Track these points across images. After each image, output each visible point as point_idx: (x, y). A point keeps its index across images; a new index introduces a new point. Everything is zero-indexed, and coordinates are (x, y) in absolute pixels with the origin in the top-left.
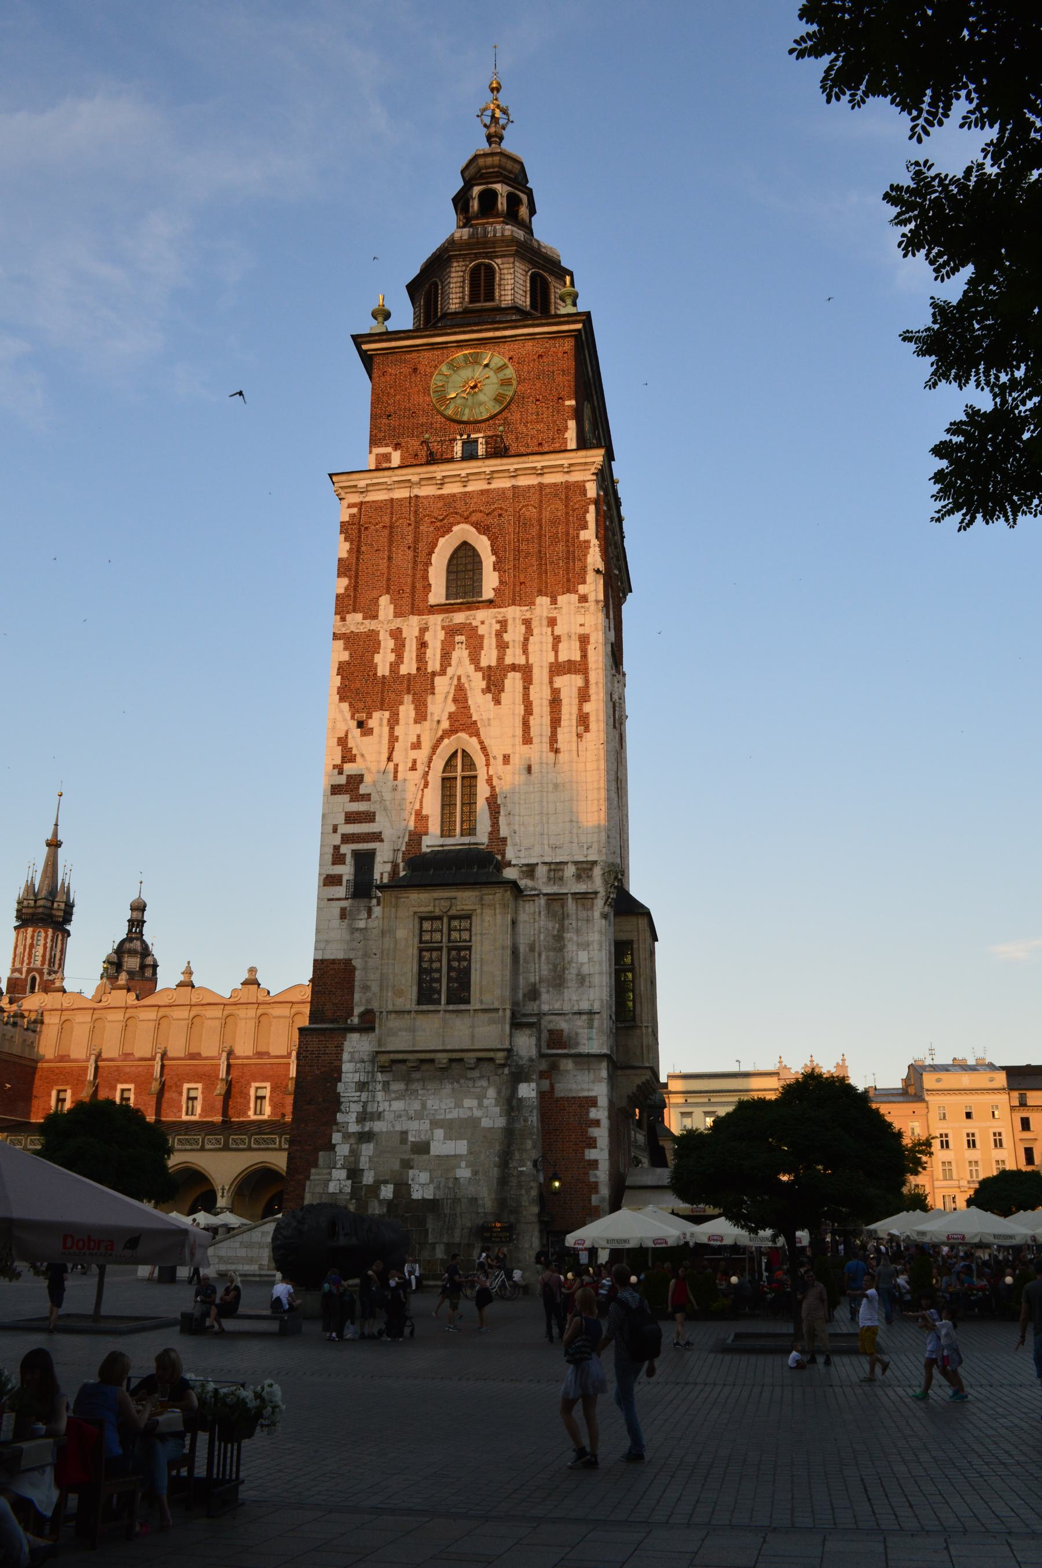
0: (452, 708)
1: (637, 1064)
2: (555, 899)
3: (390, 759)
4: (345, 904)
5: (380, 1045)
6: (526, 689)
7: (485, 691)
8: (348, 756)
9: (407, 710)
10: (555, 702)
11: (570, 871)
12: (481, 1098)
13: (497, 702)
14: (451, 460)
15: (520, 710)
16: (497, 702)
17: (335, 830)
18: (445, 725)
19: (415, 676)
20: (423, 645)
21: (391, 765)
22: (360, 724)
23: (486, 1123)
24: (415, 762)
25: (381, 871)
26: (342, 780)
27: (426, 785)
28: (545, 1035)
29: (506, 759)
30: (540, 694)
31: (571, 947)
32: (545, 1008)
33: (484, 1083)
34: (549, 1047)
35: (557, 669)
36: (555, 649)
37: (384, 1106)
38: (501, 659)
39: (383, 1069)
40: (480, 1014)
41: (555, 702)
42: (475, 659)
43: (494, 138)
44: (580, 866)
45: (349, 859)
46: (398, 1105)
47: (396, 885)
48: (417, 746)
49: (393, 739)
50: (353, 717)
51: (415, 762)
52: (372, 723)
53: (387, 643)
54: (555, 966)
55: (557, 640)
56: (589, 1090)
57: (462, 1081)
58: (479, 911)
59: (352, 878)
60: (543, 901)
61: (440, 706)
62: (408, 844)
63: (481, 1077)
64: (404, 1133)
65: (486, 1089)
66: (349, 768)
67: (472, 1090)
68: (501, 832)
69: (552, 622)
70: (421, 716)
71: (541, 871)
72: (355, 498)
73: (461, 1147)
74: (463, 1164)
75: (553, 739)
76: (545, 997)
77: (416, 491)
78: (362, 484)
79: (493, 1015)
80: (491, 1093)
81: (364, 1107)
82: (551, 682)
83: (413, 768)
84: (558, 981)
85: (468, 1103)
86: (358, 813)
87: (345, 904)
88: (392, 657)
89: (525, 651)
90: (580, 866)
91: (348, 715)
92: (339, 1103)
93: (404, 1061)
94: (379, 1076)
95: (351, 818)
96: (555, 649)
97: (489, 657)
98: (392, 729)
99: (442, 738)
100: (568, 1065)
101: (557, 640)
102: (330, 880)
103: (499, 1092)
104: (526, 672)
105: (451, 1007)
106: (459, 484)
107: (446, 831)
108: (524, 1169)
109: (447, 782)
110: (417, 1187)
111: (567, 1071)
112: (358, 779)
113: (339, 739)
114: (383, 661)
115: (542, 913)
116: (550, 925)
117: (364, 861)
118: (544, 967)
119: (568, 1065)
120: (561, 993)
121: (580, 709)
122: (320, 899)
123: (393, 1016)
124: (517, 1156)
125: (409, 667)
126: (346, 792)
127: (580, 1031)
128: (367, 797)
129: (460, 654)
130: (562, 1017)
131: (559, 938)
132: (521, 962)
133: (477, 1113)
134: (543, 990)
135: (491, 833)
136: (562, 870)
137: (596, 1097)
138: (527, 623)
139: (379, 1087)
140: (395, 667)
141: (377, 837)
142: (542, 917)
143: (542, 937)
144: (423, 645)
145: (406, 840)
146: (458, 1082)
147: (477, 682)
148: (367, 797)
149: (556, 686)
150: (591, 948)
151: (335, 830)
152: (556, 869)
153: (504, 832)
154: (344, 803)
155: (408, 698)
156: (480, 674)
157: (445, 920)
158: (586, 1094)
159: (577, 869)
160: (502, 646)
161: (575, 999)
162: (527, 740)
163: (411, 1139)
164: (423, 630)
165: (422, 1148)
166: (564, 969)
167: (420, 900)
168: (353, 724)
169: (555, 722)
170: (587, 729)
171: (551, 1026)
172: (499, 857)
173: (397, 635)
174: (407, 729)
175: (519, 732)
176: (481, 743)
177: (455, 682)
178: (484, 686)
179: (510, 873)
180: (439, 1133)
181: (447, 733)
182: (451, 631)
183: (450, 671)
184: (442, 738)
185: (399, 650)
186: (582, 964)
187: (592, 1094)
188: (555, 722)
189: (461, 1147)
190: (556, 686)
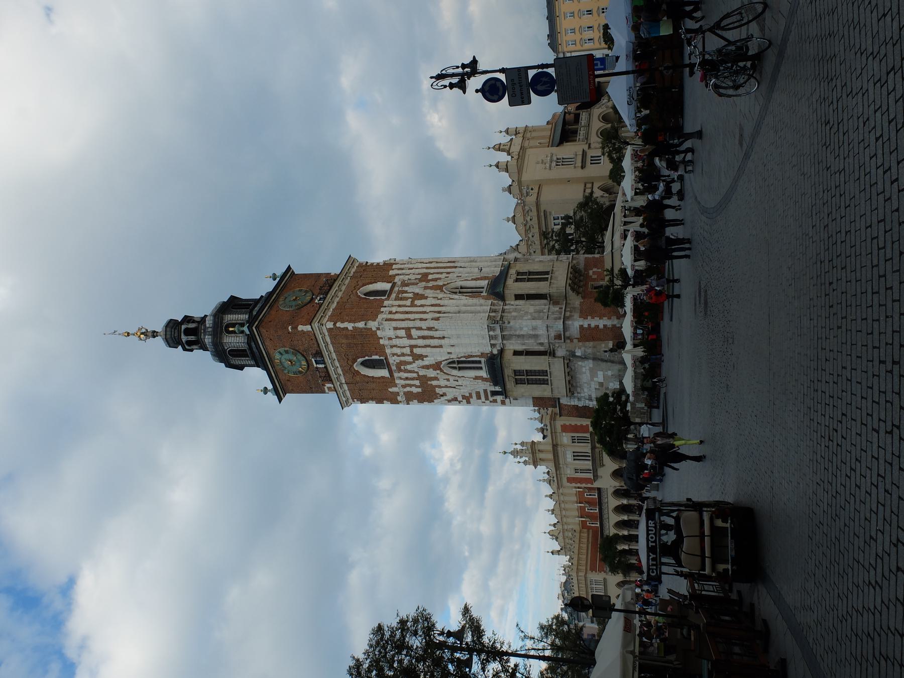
0: (431, 370)
1: (564, 294)
2: (503, 338)
3: (455, 388)
4: (511, 399)
5: (564, 396)
6: (419, 347)
7: (423, 360)
8: (455, 399)
9: (434, 383)
10: (424, 338)
11: (491, 333)
12: (582, 366)
13: (426, 356)
14: (326, 367)
15: (429, 349)
16: (426, 356)
17: (484, 402)
18: (438, 372)
19: (420, 381)
20: (407, 379)
21: (456, 387)
22: (442, 396)
23: (591, 366)
24: (454, 380)
25: (498, 389)
26: (465, 401)
27: (464, 377)
28: (557, 341)
29: (449, 353)
30: (421, 342)
31: (522, 333)
32: (546, 341)
33: (576, 365)
34: (561, 339)
35: (409, 336)
36: (401, 338)
37: (586, 394)
38: (409, 355)
39: (573, 394)
40: (551, 368)
41: (424, 338)
42: (410, 363)
43: (154, 334)
44: (490, 330)
45: (495, 397)
46: (586, 390)
47: (504, 386)
48: (448, 380)
49: (446, 387)
50: (440, 398)
51: (454, 380)
52: (441, 393)
53: (408, 389)
54: (530, 337)
55: (397, 337)
56: (577, 328)
58: (512, 368)
59: (501, 397)
60: (505, 342)
61: (431, 373)
63: (574, 366)
64: (596, 389)
66: (460, 398)
69: (390, 339)
70: (436, 379)
71: (493, 342)
72: (351, 400)
73: (600, 374)
74: (606, 373)
75: (439, 338)
77: (343, 381)
78: (344, 399)
79: (551, 364)
80: (580, 363)
81: (587, 399)
82: (416, 339)
83: (457, 381)
84: (536, 336)
85: (584, 369)
86: (477, 396)
87: (511, 399)
88: (414, 388)
89: (404, 347)
90: (490, 330)
91: (439, 400)
92: (586, 406)
93: (570, 389)
94: (576, 395)
95: (479, 397)
96: (401, 338)
97: (410, 359)
98: (442, 387)
99: (444, 372)
100: (567, 334)
101: (397, 337)
102: (503, 403)
103: (580, 361)
104: (412, 347)
105: (549, 375)
106: (337, 369)
107: (481, 368)
109: (460, 369)
110: (615, 387)
111: (570, 334)
112: (464, 397)
113: (448, 402)
114: (415, 390)
116: (514, 339)
117: (494, 393)
118: (530, 341)
119: (567, 334)
120: (540, 335)
121: (425, 330)
122: (511, 406)
123: (553, 393)
125: (417, 383)
127: (554, 330)
128: (471, 394)
129: (409, 367)
130: (549, 335)
131: (519, 336)
133: (588, 368)
134: (540, 342)
135: (480, 357)
136: (492, 336)
137: (579, 325)
138: (392, 347)
139: (579, 395)
140: (417, 387)
141: (485, 391)
143: (519, 342)
144: (407, 379)
147: (420, 363)
148: (471, 394)
149: (417, 337)
150: (522, 326)
151: (484, 402)
152: (491, 338)
154: (473, 400)
155: (429, 382)
156: (416, 361)
157: (516, 377)
158: (579, 329)
159: (491, 331)
160: (403, 355)
161: (542, 331)
162: (441, 346)
163: (598, 387)
164: (401, 378)
165: (601, 384)
166: (530, 334)
167: (510, 384)
168: (442, 397)
169: (432, 338)
170: (434, 328)
171: (553, 339)
172: (489, 355)
173: (404, 386)
174: (442, 383)
175: (438, 349)
176: (444, 361)
177: (420, 369)
178: (421, 360)
179: (495, 352)
180: (595, 379)
181: (442, 371)
182: (400, 370)
183: (416, 370)
184: (444, 372)
185: (411, 386)
186: (528, 329)
187: (578, 327)
188: (432, 338)
189: (600, 374)
190: (417, 337)
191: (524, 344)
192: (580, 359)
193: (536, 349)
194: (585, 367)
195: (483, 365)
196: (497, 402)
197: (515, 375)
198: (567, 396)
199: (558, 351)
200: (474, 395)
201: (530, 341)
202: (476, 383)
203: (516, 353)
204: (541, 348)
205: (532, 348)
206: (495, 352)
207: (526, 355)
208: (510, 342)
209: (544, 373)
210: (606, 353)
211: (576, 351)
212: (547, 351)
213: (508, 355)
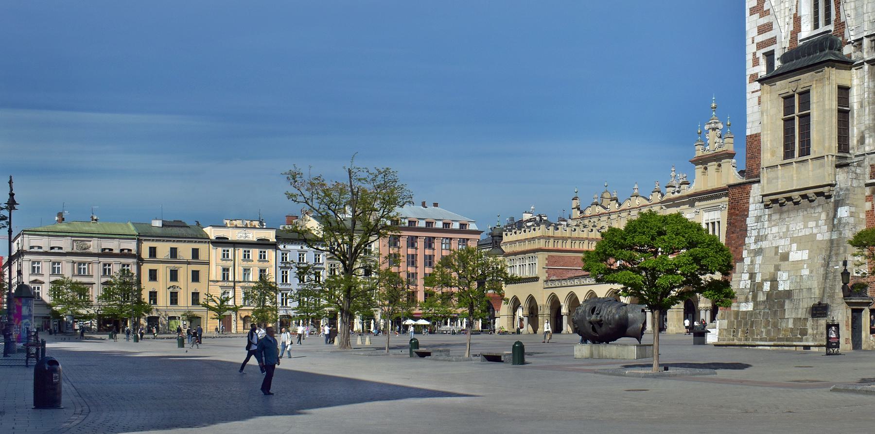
12: (817, 220)
33: (820, 210)
57: (808, 209)
62: (791, 42)
65: (820, 213)
67: (813, 215)
68: (841, 18)
76: (867, 141)
86: (764, 25)
103: (828, 215)
108: (838, 267)
115: (866, 76)
124: (834, 259)
126: (757, 11)
128: (767, 12)
132: (855, 116)
133: (815, 231)
134: (867, 136)
141: (773, 41)
142: (866, 80)
143: (866, 96)
145: (789, 38)
146: (806, 211)
148: (767, 12)
153: (842, 19)
179: (847, 50)
191: (862, 107)
192: (831, 215)
193: (853, 130)
194: (817, 226)
195: (822, 28)
196: (753, 66)
197: (800, 94)
198: (764, 196)
199: (848, 172)
200: (764, 21)
201: (867, 118)
202: (787, 20)
203: (844, 91)
204: (855, 142)
205: (855, 123)
206: (847, 50)
207: (839, 111)
208: (866, 76)
209: (805, 150)
210: (841, 263)
211: (846, 208)
212: (848, 152)
213: (837, 76)
